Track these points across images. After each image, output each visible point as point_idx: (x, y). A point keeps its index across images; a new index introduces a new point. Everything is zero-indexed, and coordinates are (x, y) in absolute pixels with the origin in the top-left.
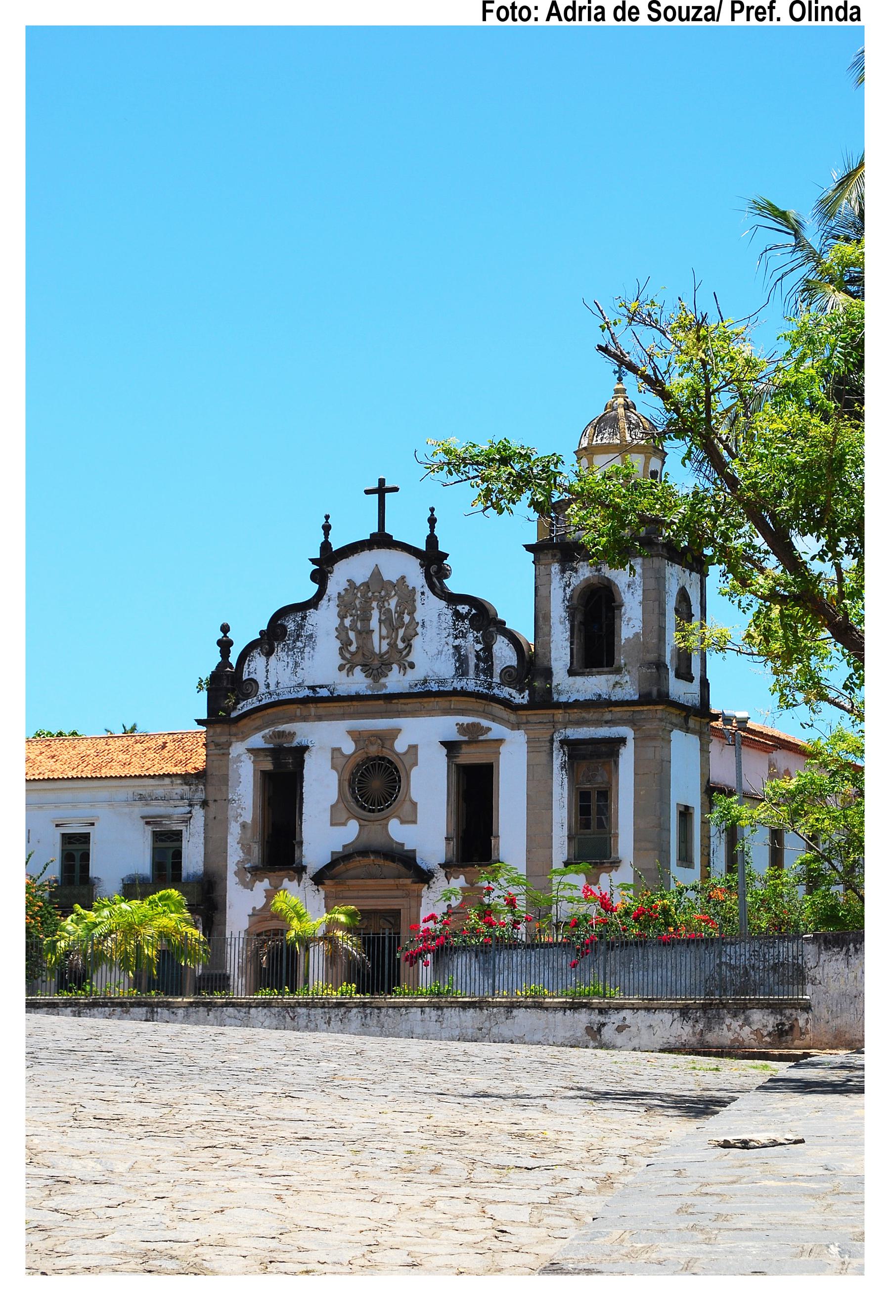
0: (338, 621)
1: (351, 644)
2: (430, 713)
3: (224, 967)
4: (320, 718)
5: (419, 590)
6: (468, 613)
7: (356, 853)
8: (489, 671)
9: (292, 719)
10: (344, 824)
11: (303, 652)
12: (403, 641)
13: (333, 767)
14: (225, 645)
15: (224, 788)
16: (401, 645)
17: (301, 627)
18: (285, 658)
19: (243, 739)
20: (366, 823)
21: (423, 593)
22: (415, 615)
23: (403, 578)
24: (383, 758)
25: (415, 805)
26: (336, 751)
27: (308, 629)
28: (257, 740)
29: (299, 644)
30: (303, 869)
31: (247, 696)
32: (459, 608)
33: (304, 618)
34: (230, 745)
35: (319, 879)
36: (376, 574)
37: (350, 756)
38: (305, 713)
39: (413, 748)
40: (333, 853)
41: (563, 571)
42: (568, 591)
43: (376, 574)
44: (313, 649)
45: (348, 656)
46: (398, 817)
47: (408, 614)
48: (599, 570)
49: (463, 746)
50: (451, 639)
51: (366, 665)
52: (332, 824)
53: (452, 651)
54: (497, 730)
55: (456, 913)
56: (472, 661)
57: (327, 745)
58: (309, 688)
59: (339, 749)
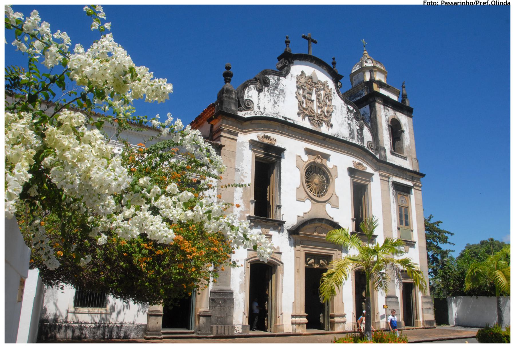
0: (296, 90)
1: (303, 103)
3: (230, 285)
5: (333, 91)
6: (353, 111)
8: (362, 140)
11: (278, 97)
12: (328, 112)
14: (228, 76)
15: (232, 160)
17: (278, 84)
21: (334, 93)
25: (338, 197)
27: (281, 86)
28: (254, 136)
29: (276, 92)
30: (281, 223)
31: (248, 108)
32: (349, 106)
33: (279, 80)
35: (293, 232)
36: (314, 73)
40: (299, 216)
41: (385, 109)
42: (387, 117)
43: (314, 73)
44: (284, 97)
45: (302, 109)
49: (358, 173)
51: (312, 117)
53: (347, 125)
54: (369, 170)
56: (356, 134)
57: (294, 153)
58: (283, 117)
59: (300, 156)
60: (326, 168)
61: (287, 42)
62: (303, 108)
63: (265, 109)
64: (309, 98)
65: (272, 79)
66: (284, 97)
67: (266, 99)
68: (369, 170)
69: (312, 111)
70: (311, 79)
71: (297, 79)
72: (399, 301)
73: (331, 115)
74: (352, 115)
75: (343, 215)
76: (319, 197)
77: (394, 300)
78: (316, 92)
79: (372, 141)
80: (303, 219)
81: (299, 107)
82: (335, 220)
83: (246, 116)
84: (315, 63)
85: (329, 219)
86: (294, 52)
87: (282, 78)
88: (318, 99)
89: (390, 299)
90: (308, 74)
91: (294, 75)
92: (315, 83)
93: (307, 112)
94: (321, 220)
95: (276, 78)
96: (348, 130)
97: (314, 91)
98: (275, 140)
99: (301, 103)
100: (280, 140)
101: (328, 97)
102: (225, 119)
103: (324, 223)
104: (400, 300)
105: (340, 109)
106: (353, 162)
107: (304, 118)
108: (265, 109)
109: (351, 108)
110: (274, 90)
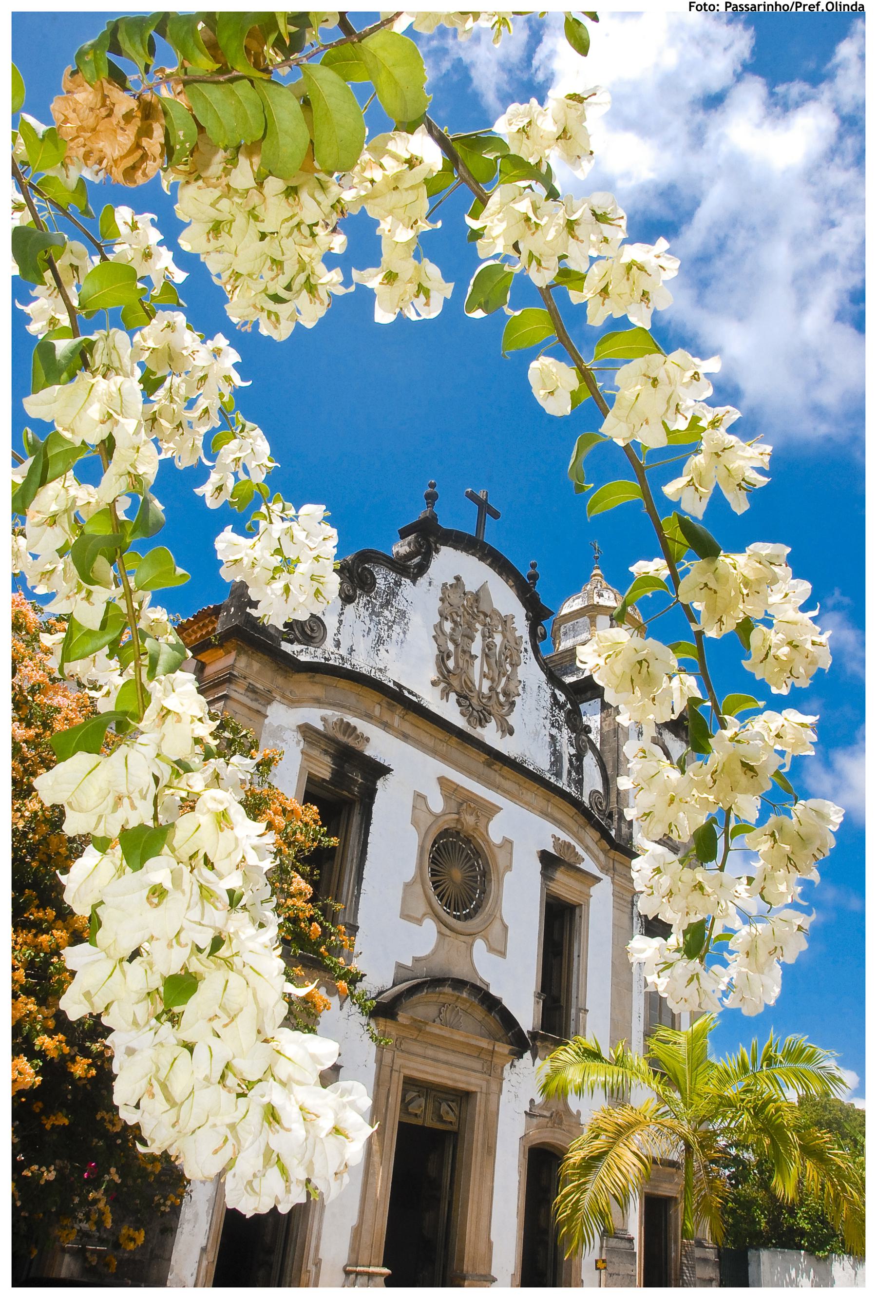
0: (438, 619)
1: (449, 657)
2: (528, 806)
4: (405, 737)
5: (524, 646)
7: (453, 980)
8: (579, 783)
9: (368, 717)
10: (419, 921)
11: (390, 628)
12: (506, 694)
13: (415, 822)
16: (502, 699)
17: (395, 594)
18: (367, 620)
19: (293, 703)
20: (448, 932)
22: (519, 669)
23: (513, 617)
24: (468, 840)
25: (506, 928)
26: (420, 797)
27: (399, 602)
29: (386, 613)
32: (557, 692)
33: (398, 584)
34: (269, 702)
35: (383, 1010)
37: (437, 817)
38: (386, 718)
39: (507, 843)
44: (404, 633)
46: (486, 939)
47: (512, 665)
48: (661, 734)
49: (562, 868)
50: (548, 724)
51: (466, 698)
52: (405, 916)
53: (548, 739)
55: (540, 1116)
56: (566, 765)
57: (412, 783)
59: (424, 798)
60: (487, 841)
61: (431, 498)
62: (449, 671)
63: (351, 650)
64: (465, 648)
65: (383, 578)
66: (404, 633)
67: (360, 627)
68: (589, 865)
69: (468, 685)
70: (477, 601)
71: (443, 593)
72: (636, 1249)
73: (513, 704)
74: (562, 716)
75: (514, 981)
76: (458, 918)
77: (624, 1245)
78: (484, 636)
79: (601, 791)
80: (409, 974)
81: (439, 667)
82: (493, 991)
83: (303, 658)
84: (490, 565)
85: (478, 983)
86: (445, 523)
87: (406, 581)
88: (487, 656)
89: (614, 1242)
90: (471, 586)
91: (434, 583)
92: (486, 615)
93: (455, 683)
94: (459, 984)
95: (392, 576)
96: (548, 752)
97: (479, 632)
98: (368, 740)
99: (443, 657)
100: (380, 744)
101: (511, 655)
102: (246, 653)
103: (465, 995)
104: (638, 1247)
105: (535, 694)
106: (554, 836)
107: (445, 695)
108: (351, 650)
109: (562, 698)
110: (382, 606)
